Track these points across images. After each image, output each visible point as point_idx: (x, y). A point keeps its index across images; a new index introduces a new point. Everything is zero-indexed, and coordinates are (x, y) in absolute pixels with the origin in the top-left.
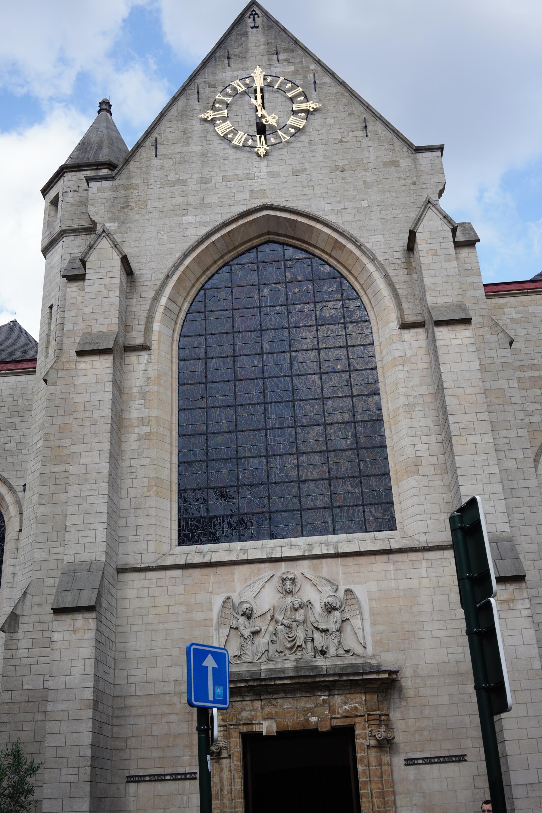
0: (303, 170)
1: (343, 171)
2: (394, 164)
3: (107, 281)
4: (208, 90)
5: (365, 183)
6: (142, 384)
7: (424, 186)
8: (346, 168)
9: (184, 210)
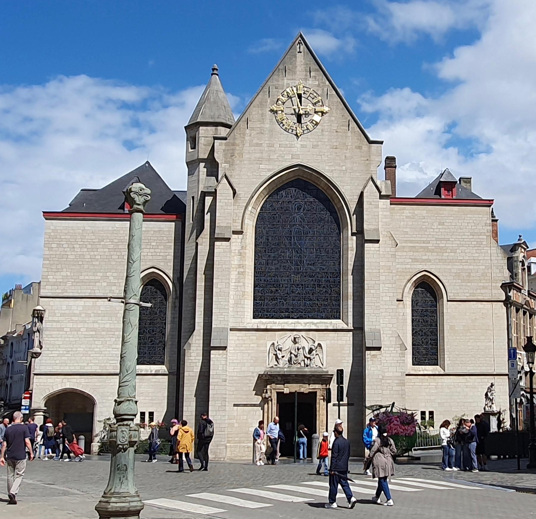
0: (318, 146)
1: (336, 148)
2: (360, 148)
3: (226, 201)
4: (275, 90)
5: (345, 157)
6: (240, 249)
7: (372, 162)
8: (338, 147)
9: (260, 161)
